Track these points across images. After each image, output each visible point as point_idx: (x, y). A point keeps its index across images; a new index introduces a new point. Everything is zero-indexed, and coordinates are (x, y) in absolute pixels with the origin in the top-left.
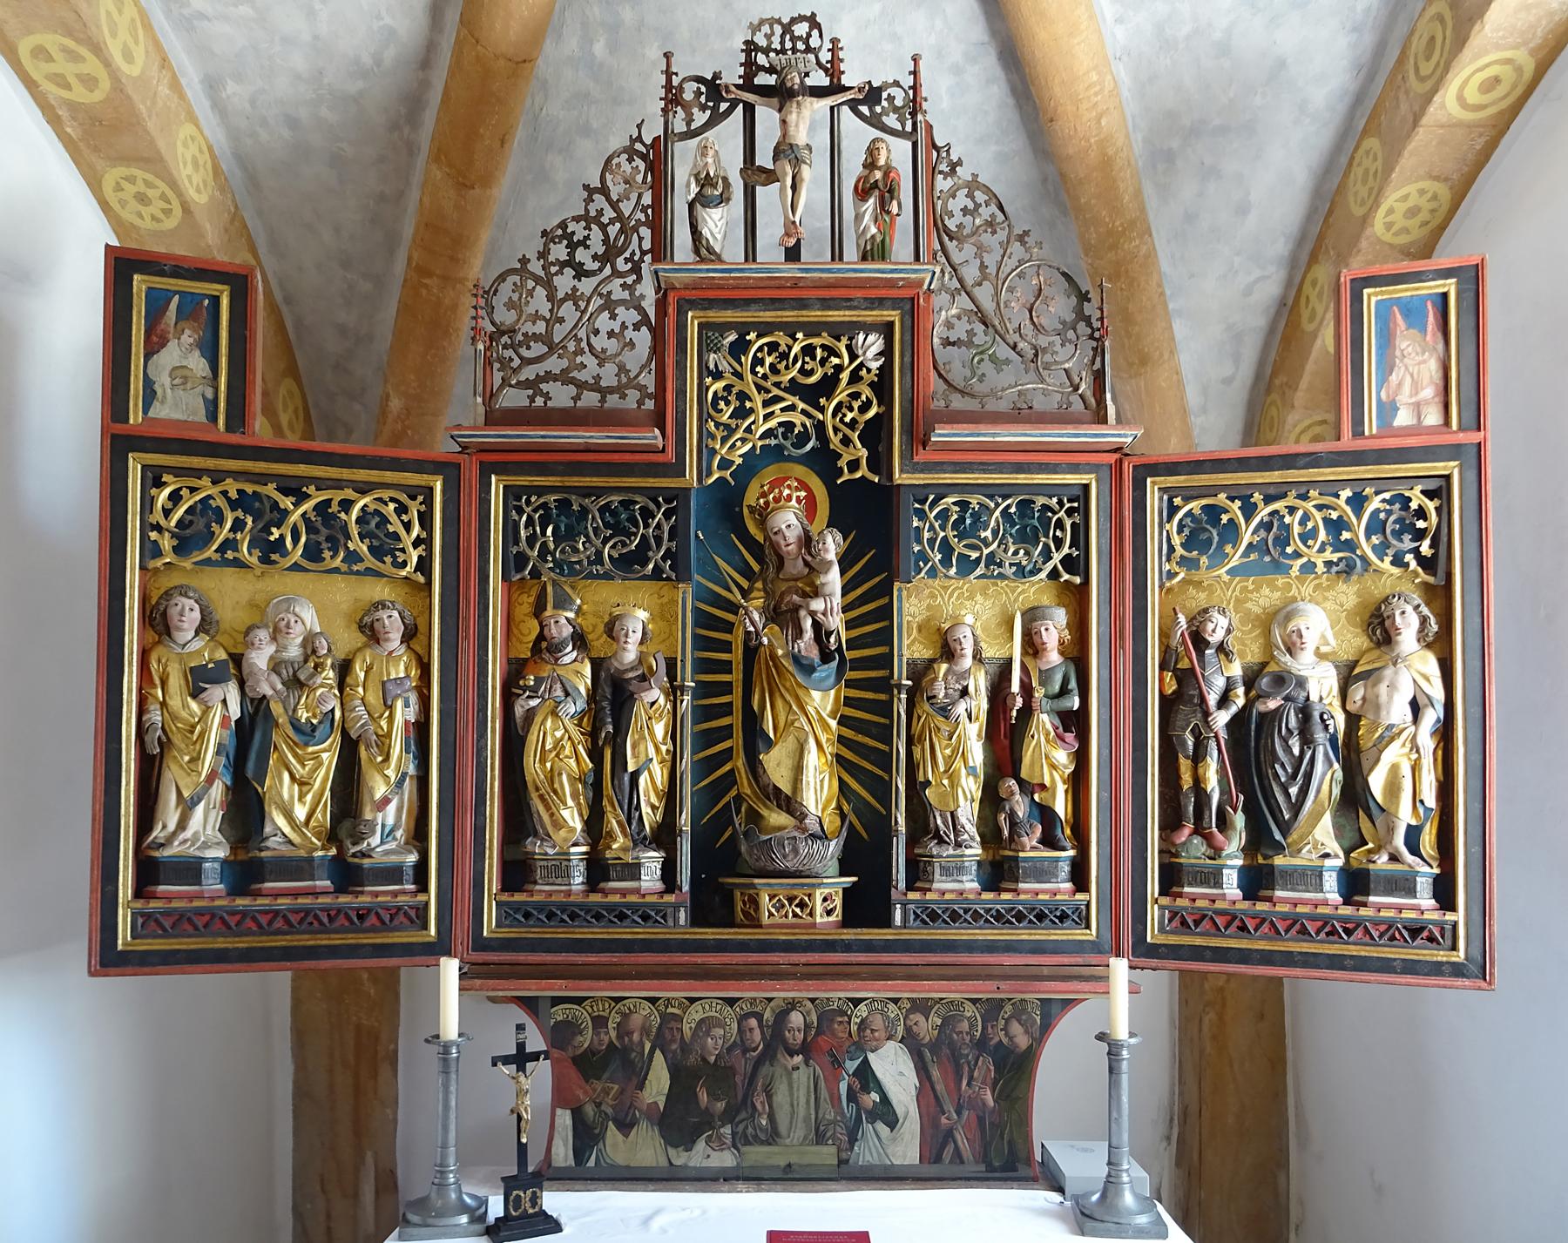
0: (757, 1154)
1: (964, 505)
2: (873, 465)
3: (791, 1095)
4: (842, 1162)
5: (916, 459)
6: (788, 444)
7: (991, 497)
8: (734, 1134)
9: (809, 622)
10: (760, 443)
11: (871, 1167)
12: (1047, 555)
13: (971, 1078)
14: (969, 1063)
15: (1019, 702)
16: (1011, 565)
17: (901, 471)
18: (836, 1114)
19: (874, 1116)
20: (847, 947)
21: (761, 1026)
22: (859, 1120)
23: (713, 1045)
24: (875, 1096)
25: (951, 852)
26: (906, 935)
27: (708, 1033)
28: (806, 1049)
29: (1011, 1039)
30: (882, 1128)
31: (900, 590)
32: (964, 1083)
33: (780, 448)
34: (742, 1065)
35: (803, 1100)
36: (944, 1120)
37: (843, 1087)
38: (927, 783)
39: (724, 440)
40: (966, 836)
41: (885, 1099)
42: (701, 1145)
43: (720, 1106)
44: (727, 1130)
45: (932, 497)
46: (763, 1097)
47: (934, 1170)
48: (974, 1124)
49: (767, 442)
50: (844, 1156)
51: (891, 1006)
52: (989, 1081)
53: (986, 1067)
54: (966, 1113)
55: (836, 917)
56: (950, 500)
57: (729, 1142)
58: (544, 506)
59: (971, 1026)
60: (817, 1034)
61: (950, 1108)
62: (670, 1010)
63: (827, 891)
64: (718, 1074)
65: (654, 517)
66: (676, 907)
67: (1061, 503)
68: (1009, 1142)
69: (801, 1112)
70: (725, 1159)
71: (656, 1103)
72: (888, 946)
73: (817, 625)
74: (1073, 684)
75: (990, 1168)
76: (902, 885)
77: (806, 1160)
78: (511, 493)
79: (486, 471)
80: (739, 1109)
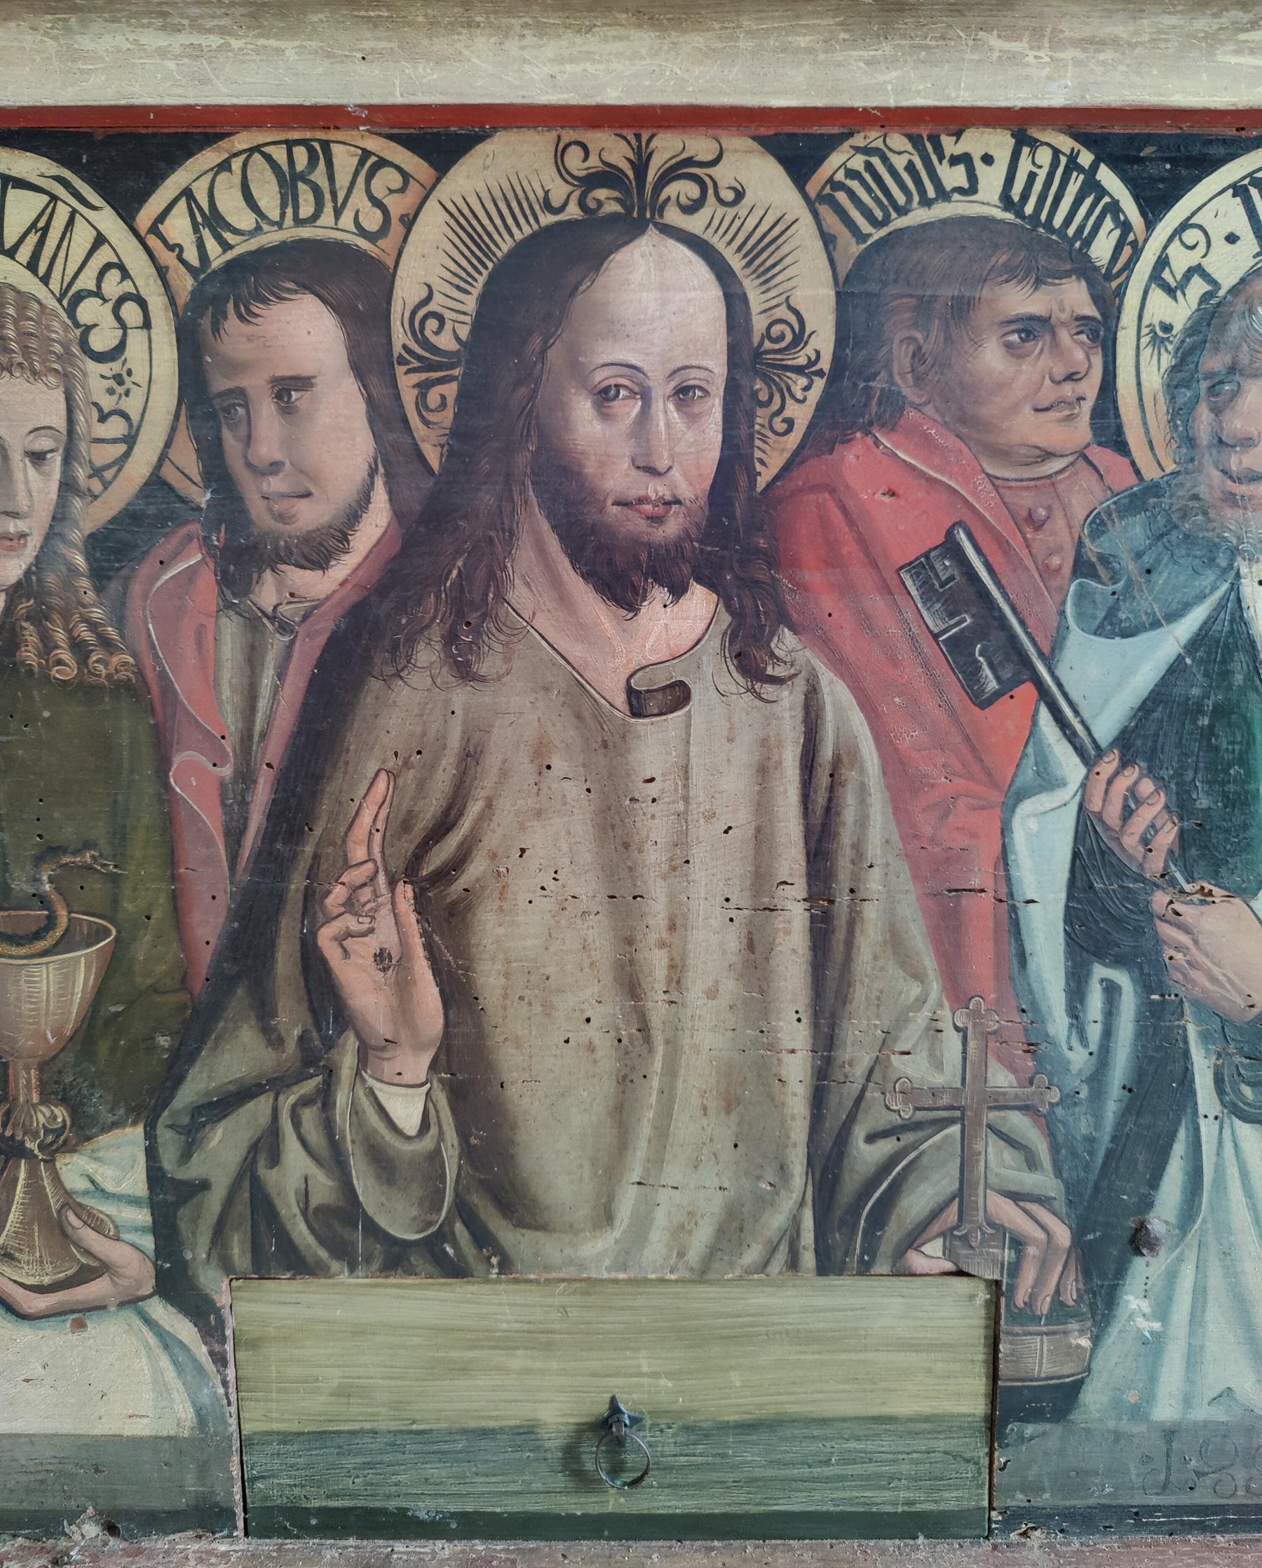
3: (623, 898)
4: (1012, 1406)
8: (169, 1197)
18: (982, 1041)
21: (371, 360)
22: (1158, 1092)
28: (739, 550)
34: (224, 679)
35: (713, 945)
37: (1041, 847)
44: (112, 1168)
46: (394, 921)
50: (1037, 1357)
57: (130, 1252)
60: (838, 420)
69: (705, 1030)
77: (736, 1390)
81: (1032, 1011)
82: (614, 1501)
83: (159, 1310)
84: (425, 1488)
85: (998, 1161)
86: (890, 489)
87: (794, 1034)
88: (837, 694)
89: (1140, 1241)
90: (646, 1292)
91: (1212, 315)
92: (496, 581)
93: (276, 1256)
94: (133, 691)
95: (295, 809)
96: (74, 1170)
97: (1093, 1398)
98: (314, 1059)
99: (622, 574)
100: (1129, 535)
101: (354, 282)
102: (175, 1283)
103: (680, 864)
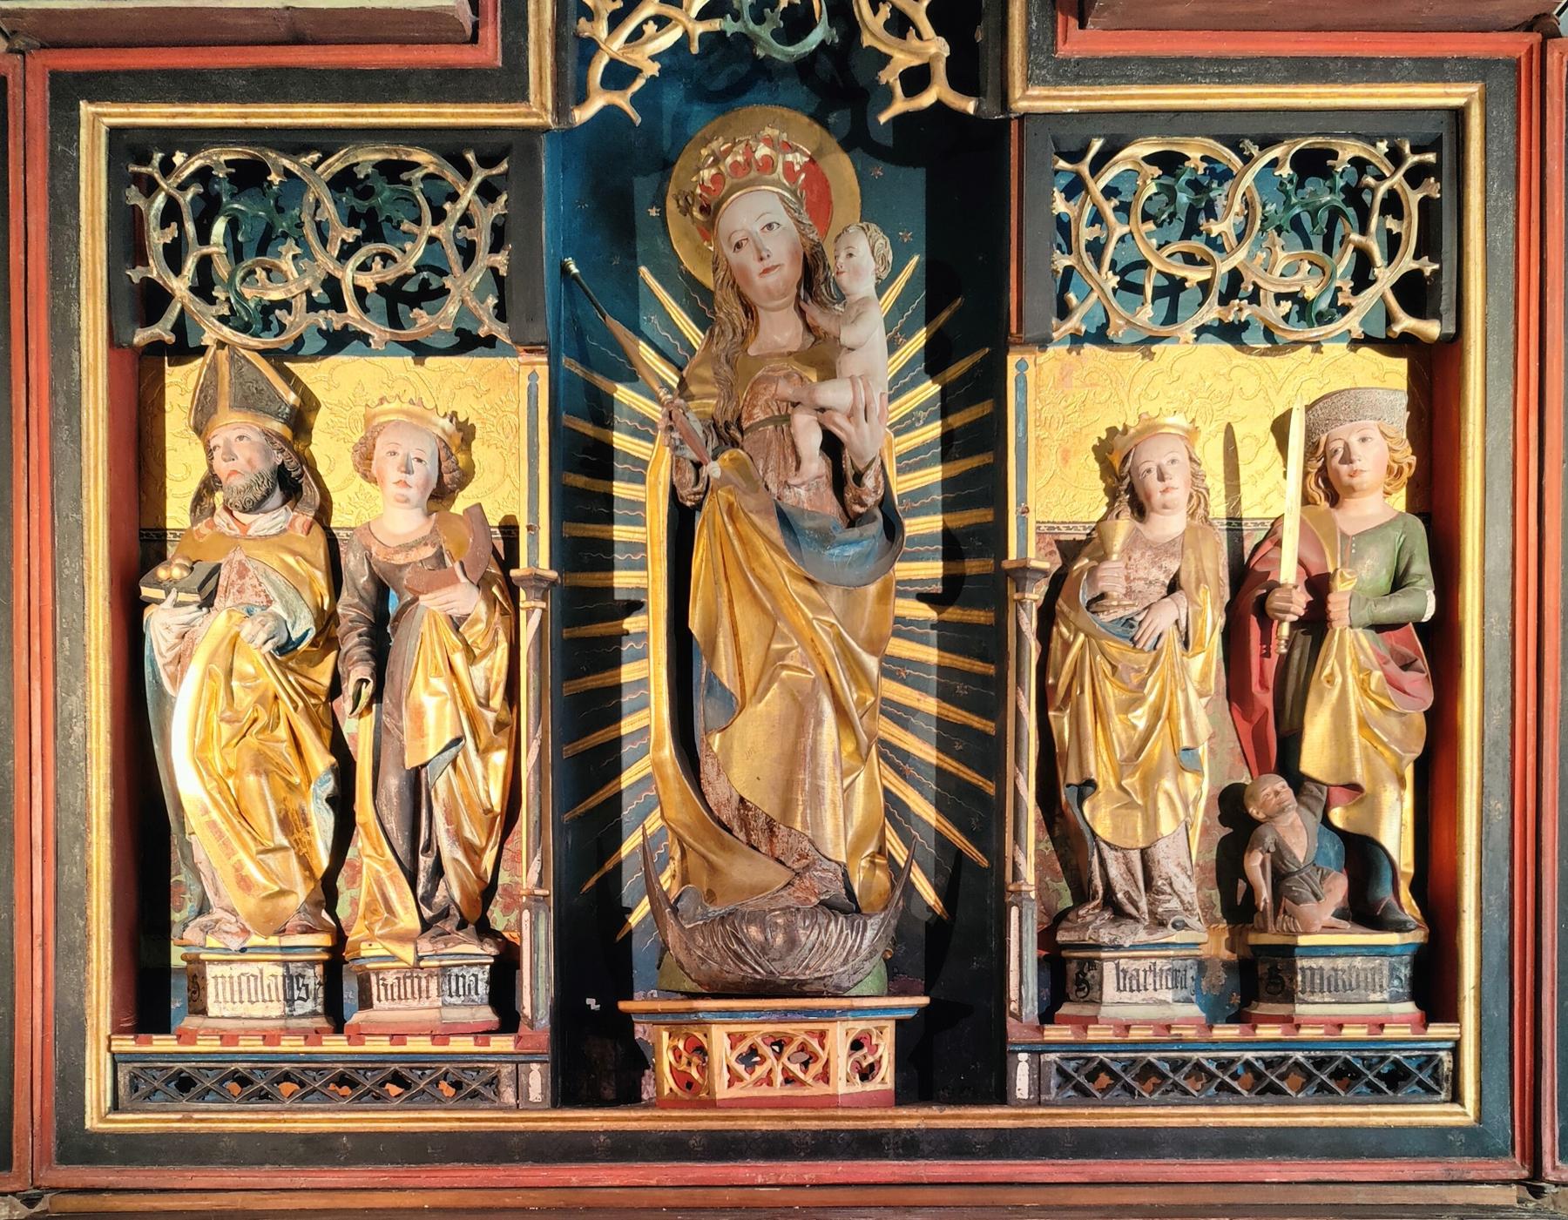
1: (1169, 162)
2: (962, 78)
5: (1063, 51)
6: (764, 32)
7: (1234, 144)
9: (817, 438)
10: (699, 29)
12: (1362, 277)
15: (1300, 601)
16: (1279, 297)
17: (1029, 80)
20: (909, 1145)
25: (1142, 936)
26: (1040, 1119)
31: (1022, 366)
33: (745, 40)
38: (1087, 786)
39: (616, 20)
40: (1174, 904)
45: (1097, 145)
49: (715, 25)
55: (886, 1077)
56: (1141, 149)
58: (204, 175)
63: (860, 1026)
65: (454, 197)
66: (519, 1061)
67: (1395, 156)
72: (1001, 1144)
73: (832, 446)
74: (1421, 566)
76: (1031, 1010)
78: (127, 147)
79: (68, 92)
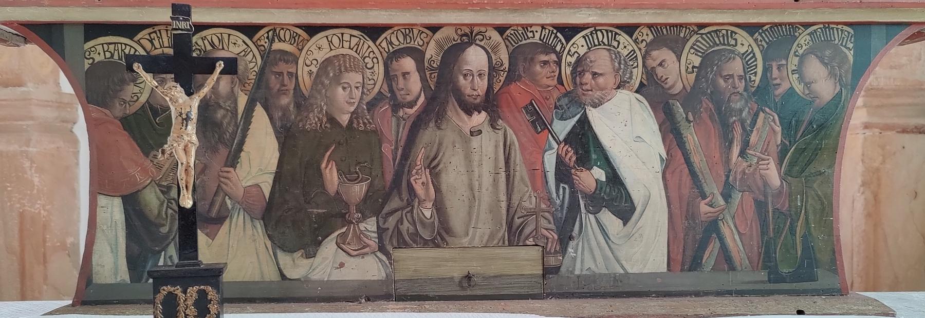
0: (416, 261)
3: (470, 171)
4: (549, 271)
8: (381, 231)
11: (593, 278)
13: (746, 145)
14: (743, 123)
19: (597, 202)
21: (421, 69)
22: (574, 208)
23: (345, 100)
24: (599, 173)
27: (337, 80)
28: (490, 104)
29: (808, 85)
30: (607, 217)
32: (736, 150)
34: (392, 130)
35: (487, 180)
36: (704, 208)
41: (614, 178)
42: (329, 248)
43: (358, 190)
44: (370, 225)
46: (425, 176)
47: (687, 280)
48: (751, 211)
50: (552, 261)
51: (623, 38)
52: (774, 149)
53: (768, 130)
54: (737, 197)
57: (373, 243)
59: (748, 67)
60: (510, 80)
61: (713, 188)
62: (277, 46)
64: (353, 141)
68: (804, 237)
70: (369, 269)
71: (257, 186)
75: (775, 277)
77: (494, 269)
80: (389, 193)
81: (549, 192)
82: (469, 293)
83: (379, 254)
84: (431, 290)
85: (543, 223)
86: (520, 92)
87: (503, 197)
88: (510, 132)
89: (571, 238)
90: (476, 248)
91: (579, 61)
92: (445, 111)
93: (402, 244)
94: (375, 132)
95: (406, 156)
96: (362, 226)
97: (563, 269)
98: (410, 204)
99: (469, 109)
100: (565, 101)
101: (417, 54)
102: (382, 249)
103: (481, 165)
